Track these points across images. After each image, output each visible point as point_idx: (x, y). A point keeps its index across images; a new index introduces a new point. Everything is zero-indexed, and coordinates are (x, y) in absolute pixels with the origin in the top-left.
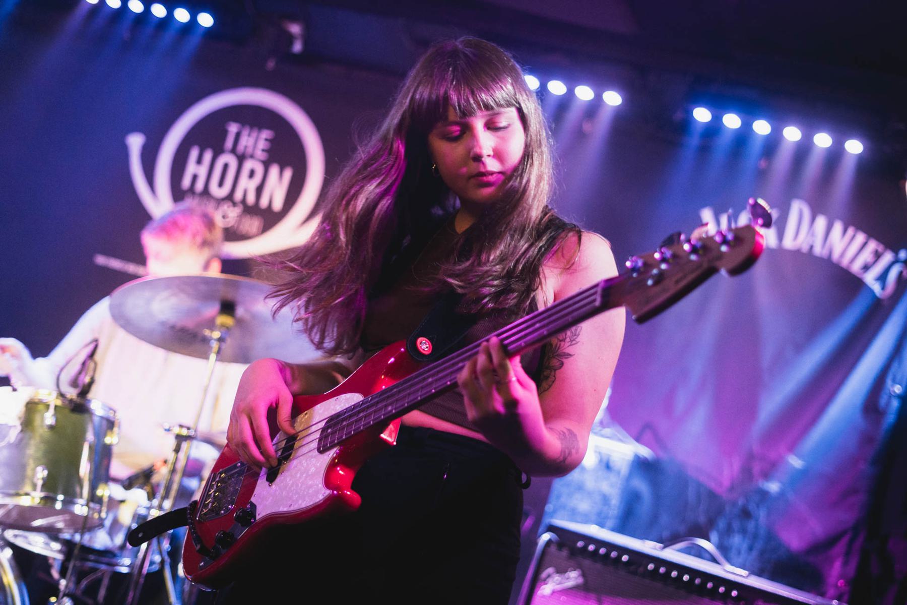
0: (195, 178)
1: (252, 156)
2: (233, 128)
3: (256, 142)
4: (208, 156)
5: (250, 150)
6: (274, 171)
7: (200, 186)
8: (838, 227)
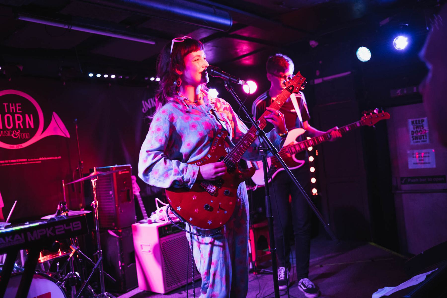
1: (17, 113)
3: (16, 107)
5: (15, 111)
6: (27, 115)
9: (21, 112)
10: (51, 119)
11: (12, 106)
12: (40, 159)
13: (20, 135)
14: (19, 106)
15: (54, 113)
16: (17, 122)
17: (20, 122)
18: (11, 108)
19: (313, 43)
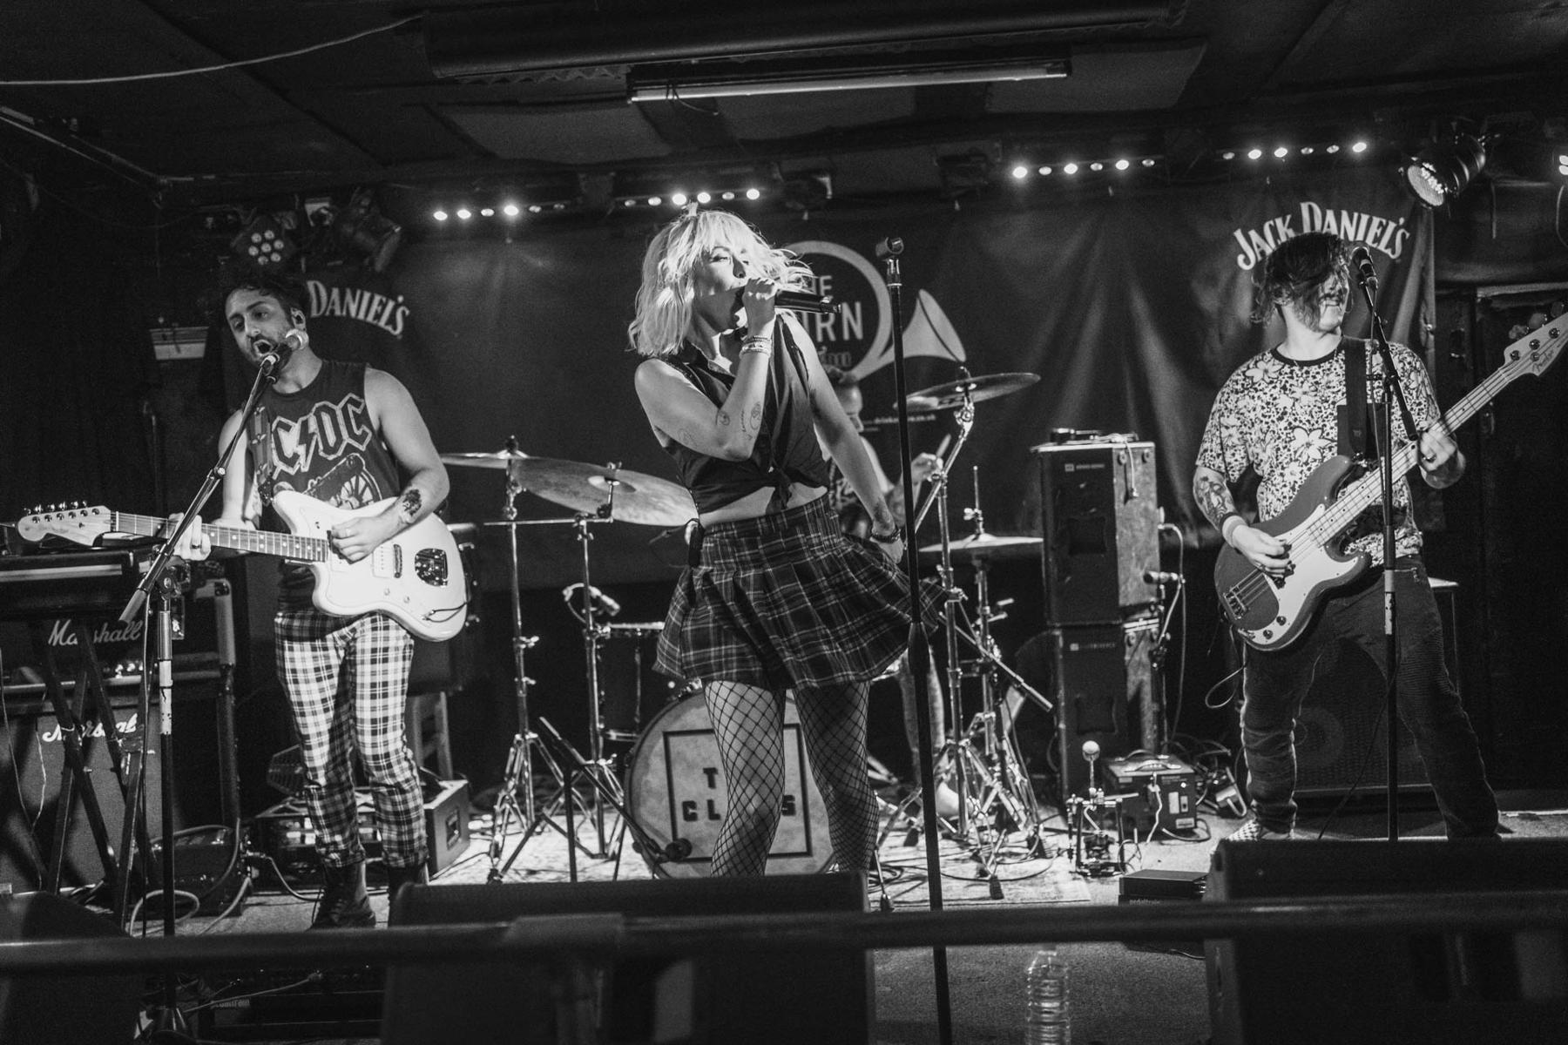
8: (1345, 214)
10: (913, 309)
12: (877, 421)
14: (826, 283)
15: (923, 294)
17: (828, 325)
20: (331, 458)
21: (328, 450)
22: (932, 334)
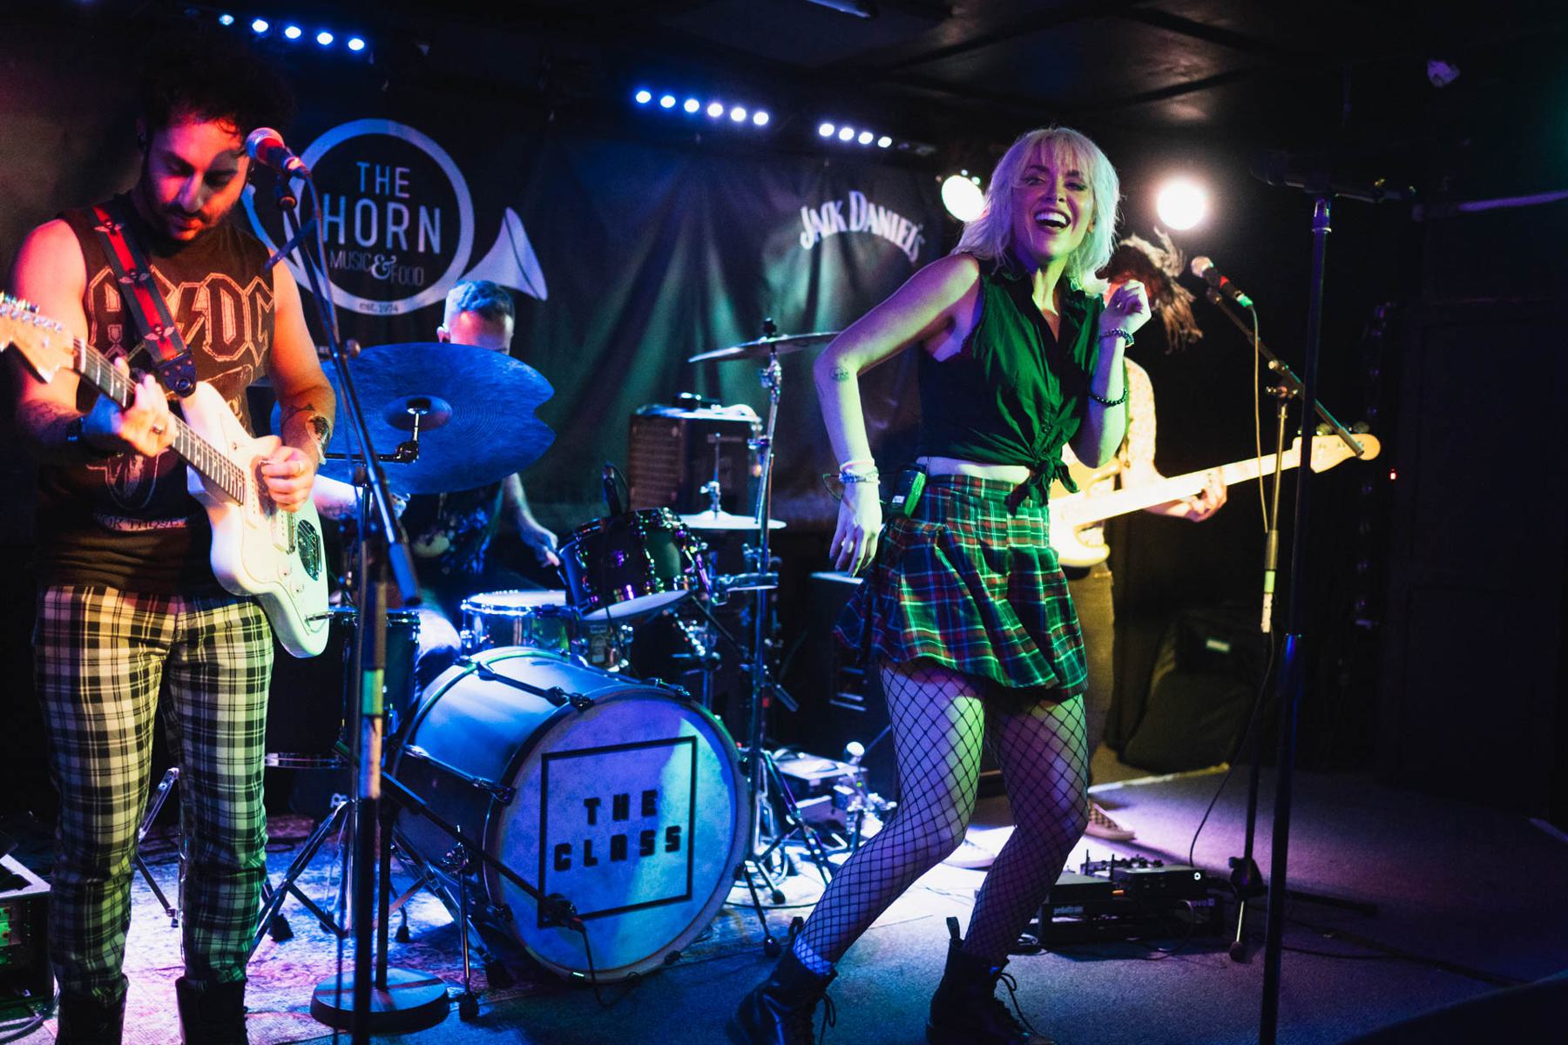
0: (333, 228)
2: (363, 165)
4: (343, 201)
6: (423, 212)
7: (342, 240)
9: (406, 195)
11: (383, 175)
13: (396, 270)
14: (403, 176)
15: (511, 214)
16: (391, 228)
17: (401, 230)
18: (379, 179)
19: (1442, 72)
20: (220, 359)
21: (219, 346)
22: (515, 265)
